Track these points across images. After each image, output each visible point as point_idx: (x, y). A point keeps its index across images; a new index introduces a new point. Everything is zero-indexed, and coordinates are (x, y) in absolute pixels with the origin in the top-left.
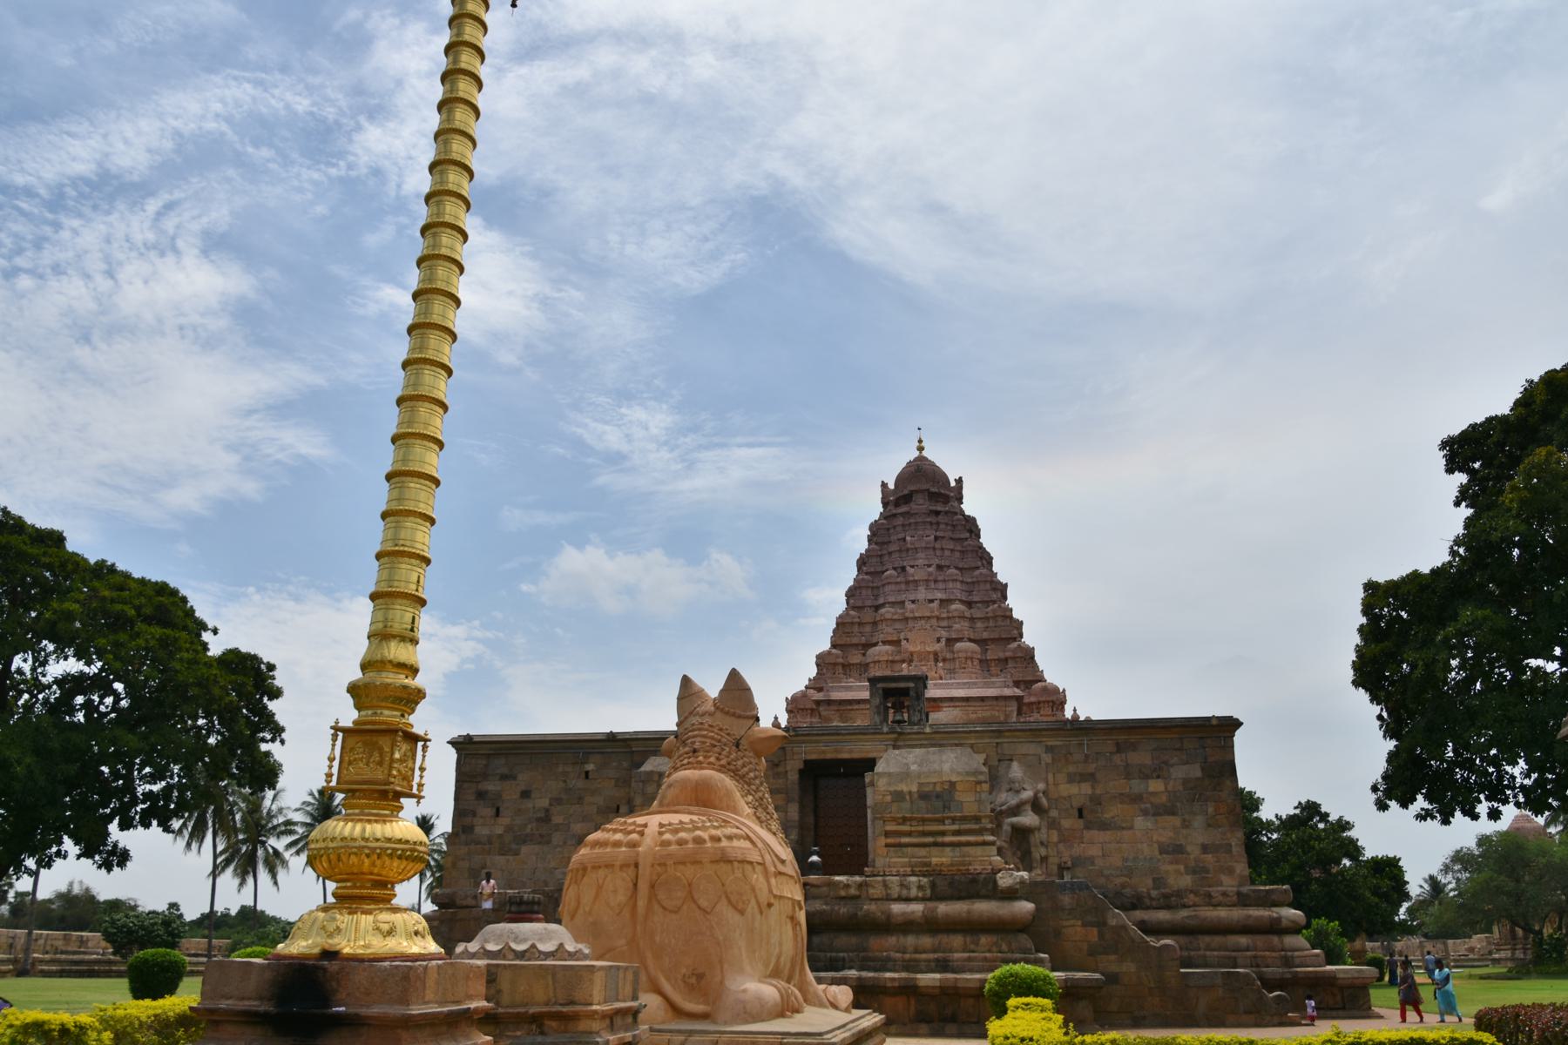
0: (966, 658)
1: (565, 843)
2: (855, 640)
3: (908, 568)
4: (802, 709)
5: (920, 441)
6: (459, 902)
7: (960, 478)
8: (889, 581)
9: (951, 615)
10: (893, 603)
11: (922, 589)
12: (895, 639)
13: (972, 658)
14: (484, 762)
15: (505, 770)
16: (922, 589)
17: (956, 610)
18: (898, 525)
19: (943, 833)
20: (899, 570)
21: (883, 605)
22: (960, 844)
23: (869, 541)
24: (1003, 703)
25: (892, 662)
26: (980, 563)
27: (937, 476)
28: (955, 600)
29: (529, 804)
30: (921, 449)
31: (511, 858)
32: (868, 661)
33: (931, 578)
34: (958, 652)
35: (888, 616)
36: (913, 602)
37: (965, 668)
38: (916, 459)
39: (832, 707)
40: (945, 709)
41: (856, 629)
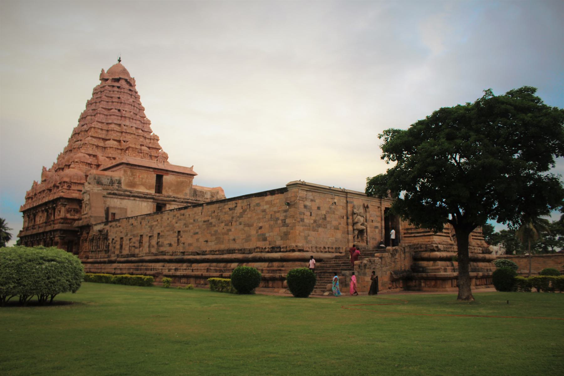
0: (146, 153)
1: (331, 228)
2: (100, 136)
4: (82, 162)
6: (305, 249)
8: (114, 114)
9: (139, 134)
10: (116, 124)
11: (127, 121)
12: (118, 139)
14: (306, 193)
15: (311, 197)
16: (127, 121)
18: (116, 91)
21: (110, 124)
24: (189, 176)
25: (118, 149)
29: (320, 212)
30: (120, 61)
31: (316, 233)
32: (106, 146)
33: (132, 117)
34: (143, 150)
35: (115, 129)
36: (125, 125)
38: (116, 64)
39: (128, 166)
40: (170, 175)
41: (99, 131)
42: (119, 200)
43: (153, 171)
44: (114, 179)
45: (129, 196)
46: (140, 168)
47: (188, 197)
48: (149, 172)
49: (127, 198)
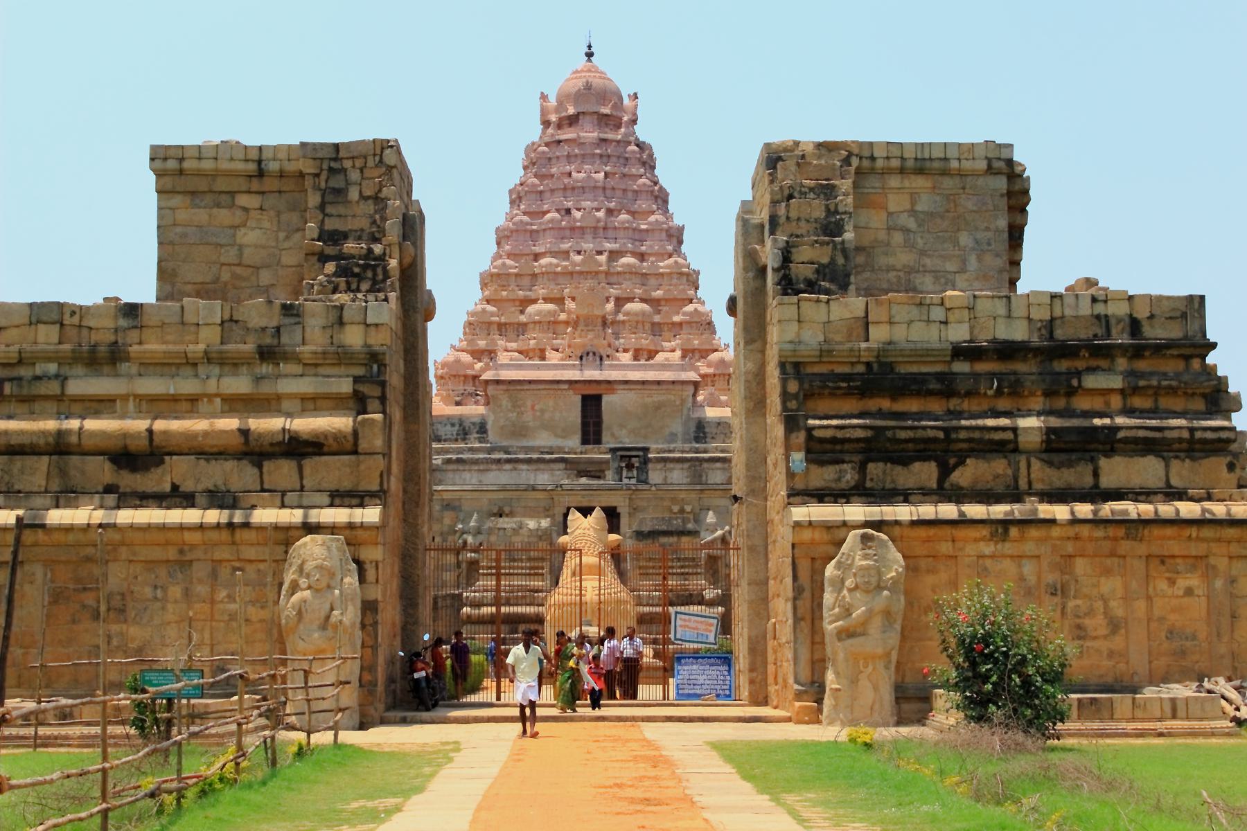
0: (637, 322)
3: (574, 212)
4: (455, 376)
5: (590, 47)
7: (635, 94)
11: (589, 237)
12: (558, 296)
13: (643, 322)
16: (589, 237)
17: (628, 265)
19: (672, 567)
20: (563, 213)
21: (543, 255)
22: (682, 574)
23: (525, 168)
24: (679, 387)
25: (556, 322)
26: (655, 207)
27: (609, 95)
28: (626, 252)
30: (590, 55)
36: (579, 253)
37: (635, 333)
39: (501, 387)
42: (475, 474)
43: (569, 389)
44: (467, 424)
45: (499, 461)
46: (533, 386)
47: (679, 445)
48: (559, 392)
49: (494, 467)
